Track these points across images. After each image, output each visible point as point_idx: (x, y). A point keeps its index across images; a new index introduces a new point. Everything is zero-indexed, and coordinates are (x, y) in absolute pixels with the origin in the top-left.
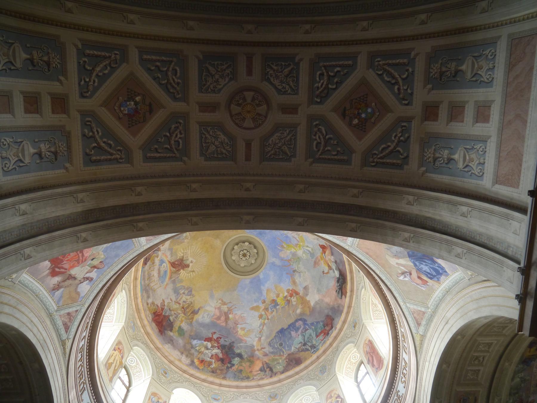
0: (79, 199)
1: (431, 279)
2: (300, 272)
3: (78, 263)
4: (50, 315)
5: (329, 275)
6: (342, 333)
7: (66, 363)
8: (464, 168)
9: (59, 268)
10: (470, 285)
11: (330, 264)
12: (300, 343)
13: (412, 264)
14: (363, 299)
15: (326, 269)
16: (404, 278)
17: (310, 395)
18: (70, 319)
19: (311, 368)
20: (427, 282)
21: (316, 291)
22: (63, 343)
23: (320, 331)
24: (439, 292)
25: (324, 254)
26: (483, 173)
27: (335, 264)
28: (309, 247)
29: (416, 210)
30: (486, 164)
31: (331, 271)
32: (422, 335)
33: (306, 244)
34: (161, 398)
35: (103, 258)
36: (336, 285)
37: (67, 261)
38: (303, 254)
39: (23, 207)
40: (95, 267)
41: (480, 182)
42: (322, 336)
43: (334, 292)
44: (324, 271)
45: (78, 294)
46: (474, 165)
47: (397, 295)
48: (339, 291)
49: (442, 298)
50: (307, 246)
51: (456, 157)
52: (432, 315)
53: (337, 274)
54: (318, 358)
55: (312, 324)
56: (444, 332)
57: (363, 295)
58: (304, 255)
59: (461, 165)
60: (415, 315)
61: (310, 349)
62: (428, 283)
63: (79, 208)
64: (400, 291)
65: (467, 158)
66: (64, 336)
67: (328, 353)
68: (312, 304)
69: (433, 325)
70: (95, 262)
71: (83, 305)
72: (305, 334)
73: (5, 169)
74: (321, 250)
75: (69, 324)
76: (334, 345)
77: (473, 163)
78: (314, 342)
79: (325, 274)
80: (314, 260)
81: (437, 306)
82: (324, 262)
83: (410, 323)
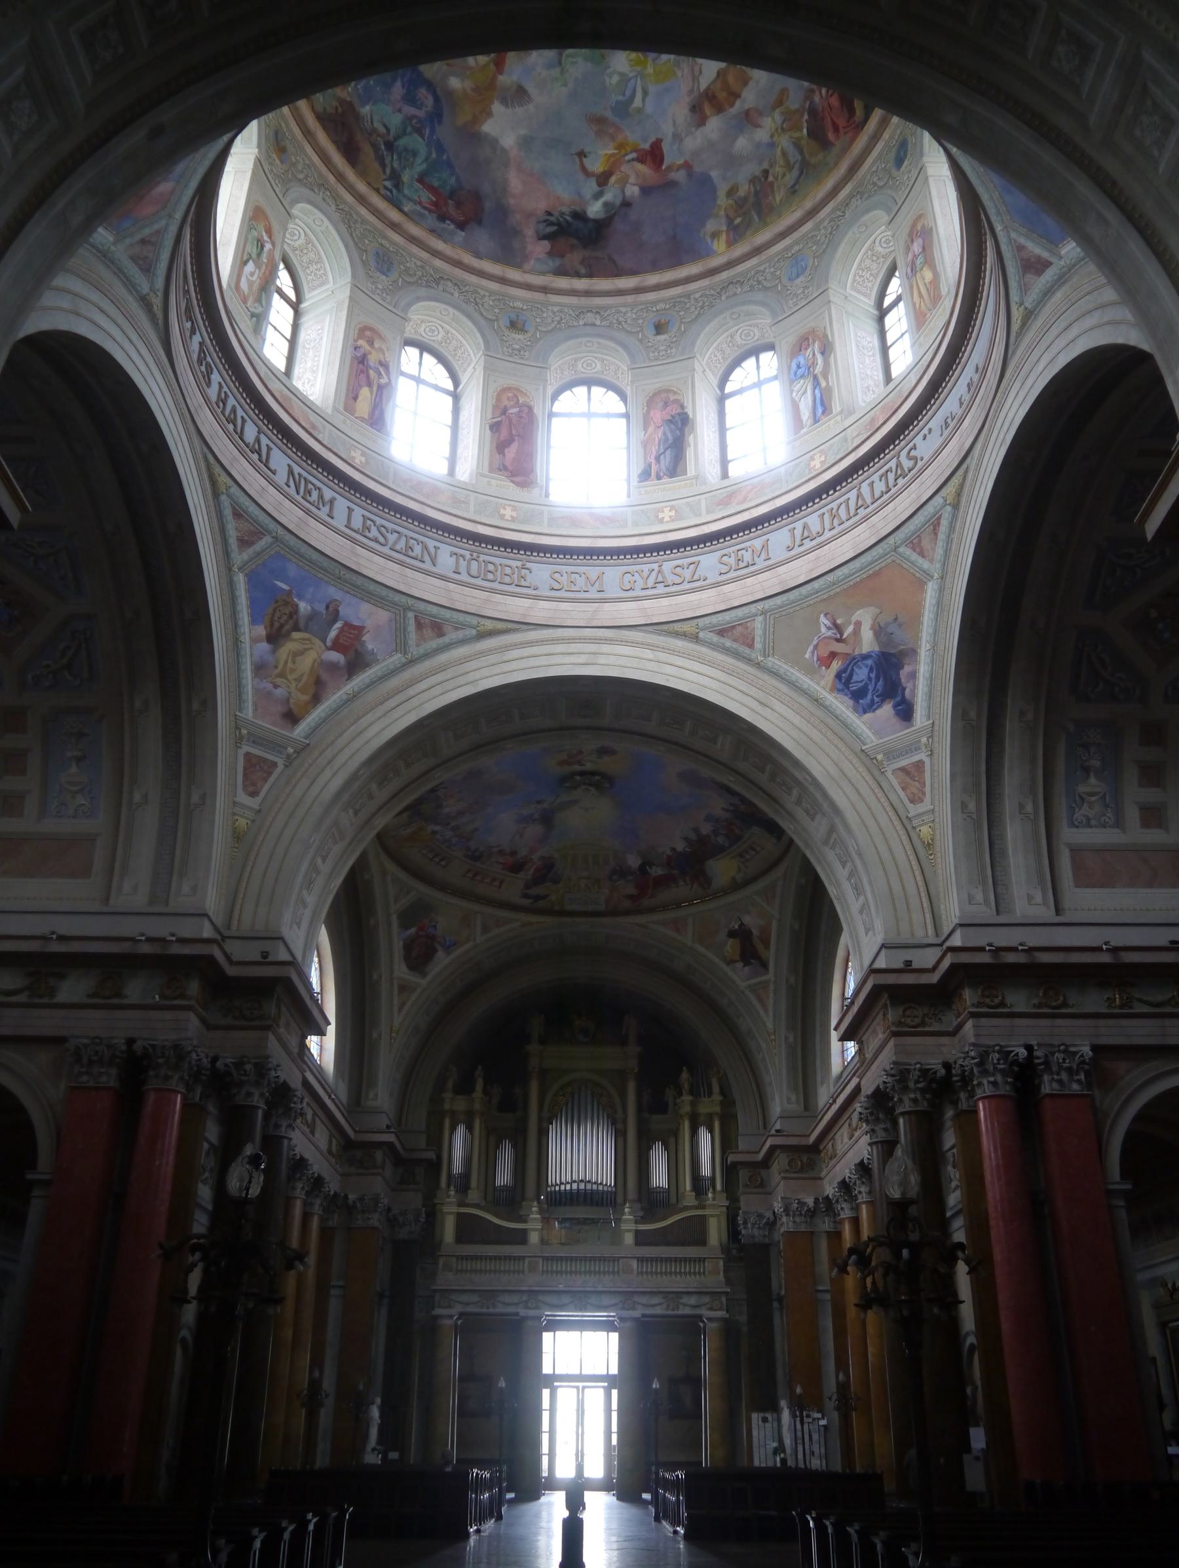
1: (838, 676)
2: (560, 63)
5: (581, 176)
6: (473, 279)
8: (1079, 795)
10: (856, 754)
11: (613, 179)
12: (385, 126)
13: (864, 651)
14: (589, 341)
15: (597, 165)
16: (825, 625)
17: (308, 241)
19: (363, 211)
20: (828, 667)
21: (523, 132)
23: (436, 184)
24: (809, 685)
25: (634, 155)
26: (1078, 827)
27: (618, 202)
28: (644, 100)
29: (1012, 728)
30: (1089, 830)
31: (591, 186)
32: (697, 637)
33: (652, 89)
36: (565, 209)
38: (622, 75)
41: (1065, 822)
42: (429, 198)
43: (541, 206)
44: (585, 156)
46: (1085, 810)
47: (778, 600)
48: (552, 224)
49: (799, 688)
50: (645, 93)
51: (1093, 780)
52: (749, 660)
53: (595, 210)
54: (394, 226)
55: (440, 148)
56: (739, 696)
57: (599, 343)
58: (615, 79)
59: (1082, 789)
60: (740, 629)
61: (388, 170)
62: (824, 668)
64: (791, 611)
65: (1093, 799)
67: (415, 250)
68: (488, 127)
69: (730, 660)
72: (410, 134)
74: (647, 146)
76: (438, 263)
77: (1088, 809)
78: (405, 178)
79: (577, 160)
80: (608, 114)
81: (774, 673)
82: (613, 155)
83: (720, 617)
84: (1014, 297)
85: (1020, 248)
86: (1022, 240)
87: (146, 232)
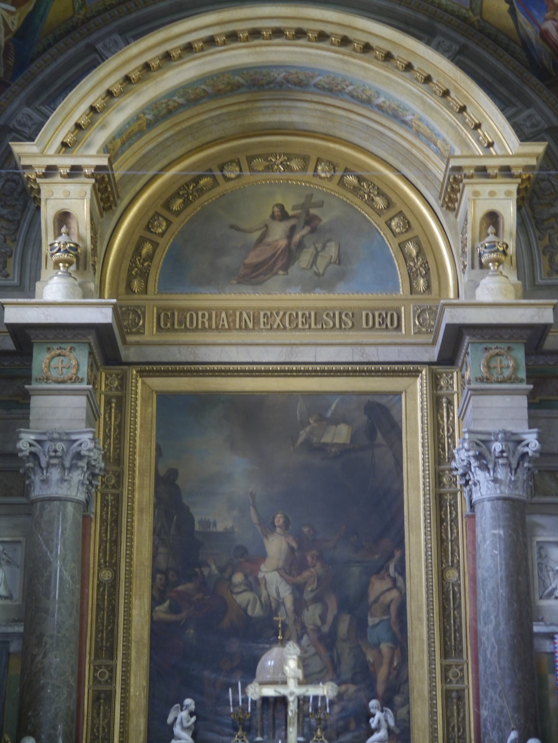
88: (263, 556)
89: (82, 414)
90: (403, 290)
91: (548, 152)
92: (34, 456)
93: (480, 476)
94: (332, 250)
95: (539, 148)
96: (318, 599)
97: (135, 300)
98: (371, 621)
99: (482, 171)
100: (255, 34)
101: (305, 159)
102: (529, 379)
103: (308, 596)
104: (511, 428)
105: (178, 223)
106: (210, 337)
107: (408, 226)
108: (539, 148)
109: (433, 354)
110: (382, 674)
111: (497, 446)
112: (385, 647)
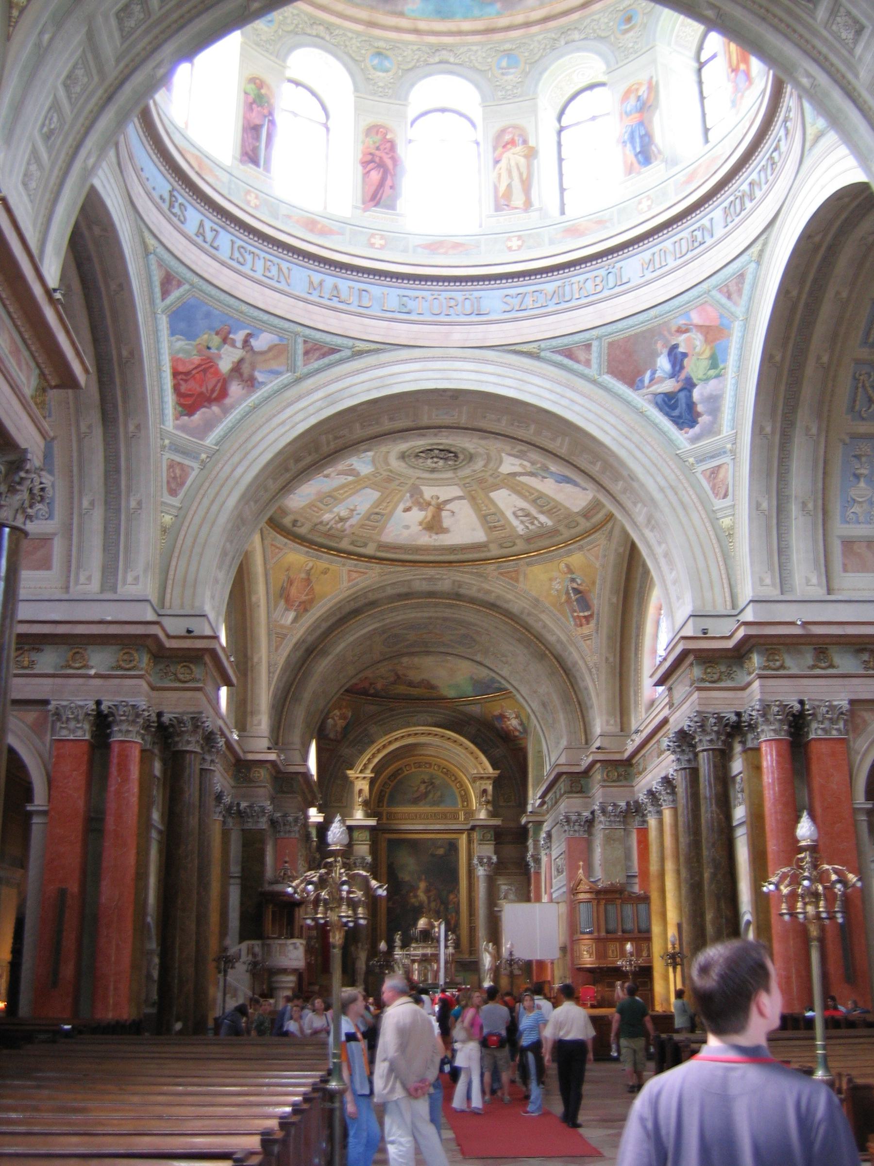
0: (87, 431)
3: (211, 367)
4: (298, 380)
7: (396, 347)
9: (213, 391)
18: (316, 350)
22: (359, 354)
34: (640, 84)
35: (210, 335)
37: (201, 386)
39: (85, 504)
40: (225, 340)
45: (270, 349)
63: (98, 432)
66: (347, 353)
70: (216, 340)
71: (297, 334)
73: (47, 516)
75: (325, 349)
84: (160, 250)
85: (180, 284)
86: (182, 290)
87: (724, 300)
88: (418, 888)
89: (368, 850)
90: (460, 806)
91: (500, 776)
92: (355, 863)
93: (480, 868)
94: (439, 794)
95: (498, 772)
96: (434, 900)
97: (380, 809)
98: (450, 907)
99: (482, 778)
100: (416, 734)
101: (430, 764)
102: (495, 840)
103: (432, 899)
104: (489, 854)
105: (392, 784)
106: (403, 822)
107: (462, 786)
108: (498, 772)
109: (468, 827)
110: (453, 922)
111: (485, 860)
112: (454, 914)
